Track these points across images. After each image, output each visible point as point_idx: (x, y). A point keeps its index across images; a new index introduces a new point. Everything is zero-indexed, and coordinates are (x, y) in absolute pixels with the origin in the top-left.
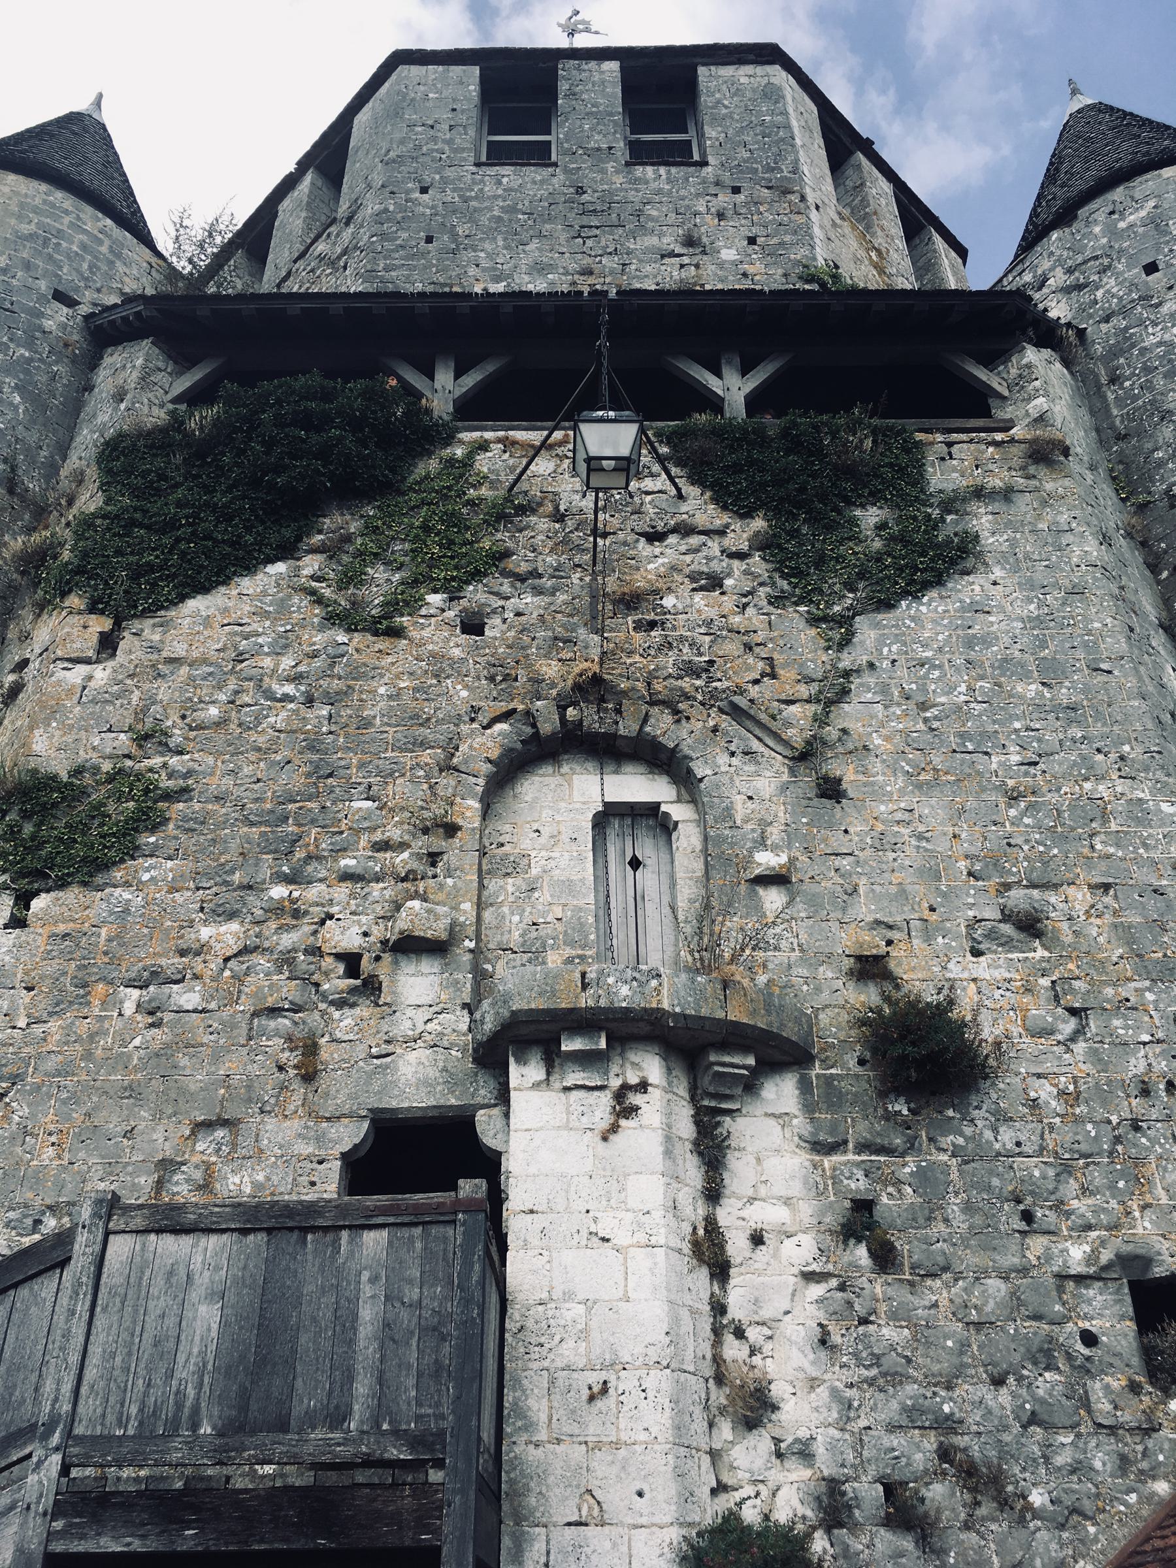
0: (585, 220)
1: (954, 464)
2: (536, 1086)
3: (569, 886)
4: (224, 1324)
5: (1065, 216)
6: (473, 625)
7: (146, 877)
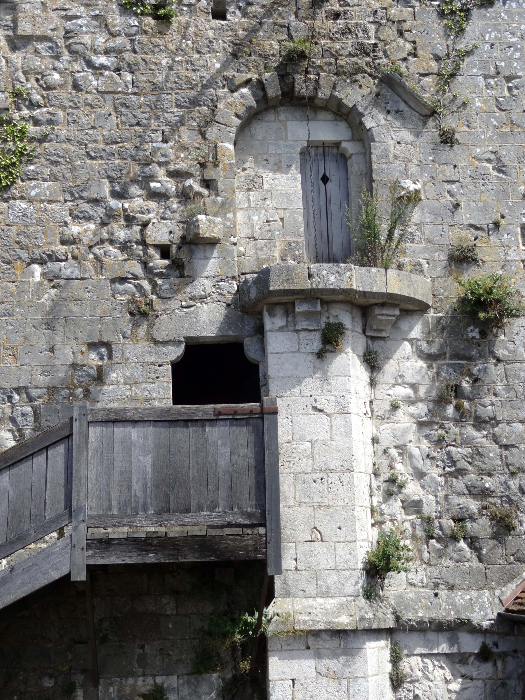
2: (281, 329)
3: (287, 196)
4: (153, 464)
7: (33, 193)
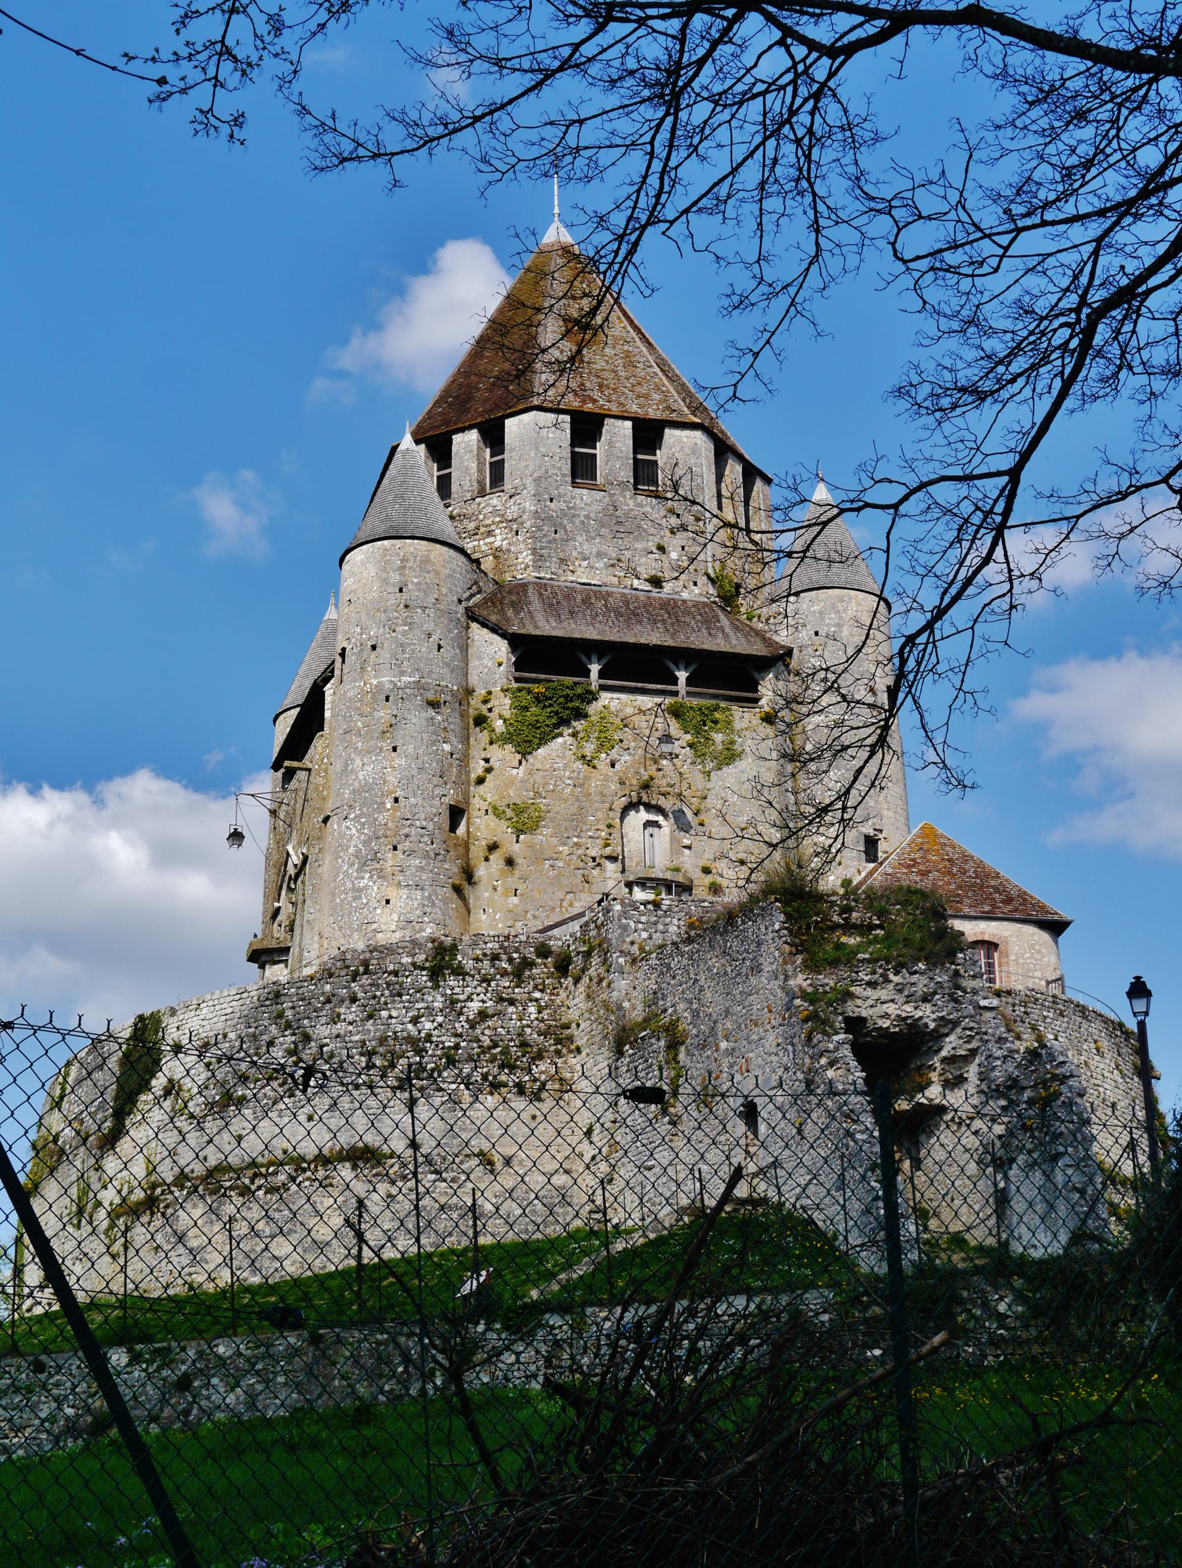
0: (617, 528)
1: (743, 718)
6: (613, 766)
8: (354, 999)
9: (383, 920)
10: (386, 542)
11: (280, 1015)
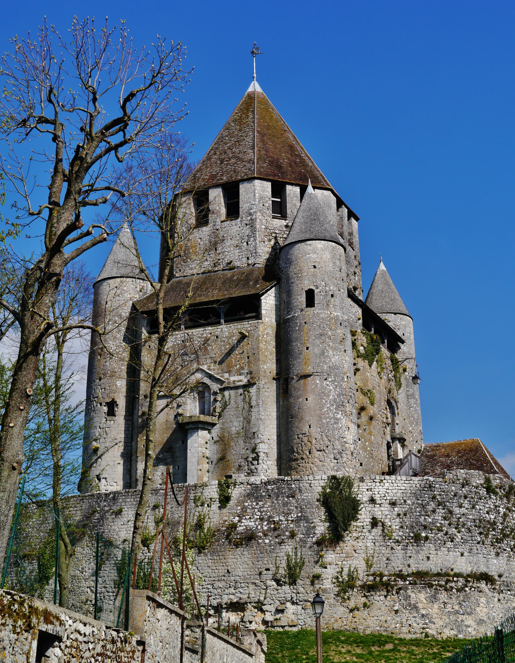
5: (395, 314)
8: (466, 497)
9: (348, 437)
10: (334, 244)
11: (434, 498)
